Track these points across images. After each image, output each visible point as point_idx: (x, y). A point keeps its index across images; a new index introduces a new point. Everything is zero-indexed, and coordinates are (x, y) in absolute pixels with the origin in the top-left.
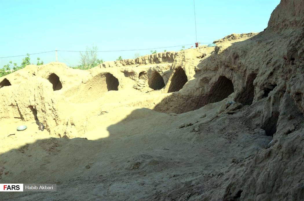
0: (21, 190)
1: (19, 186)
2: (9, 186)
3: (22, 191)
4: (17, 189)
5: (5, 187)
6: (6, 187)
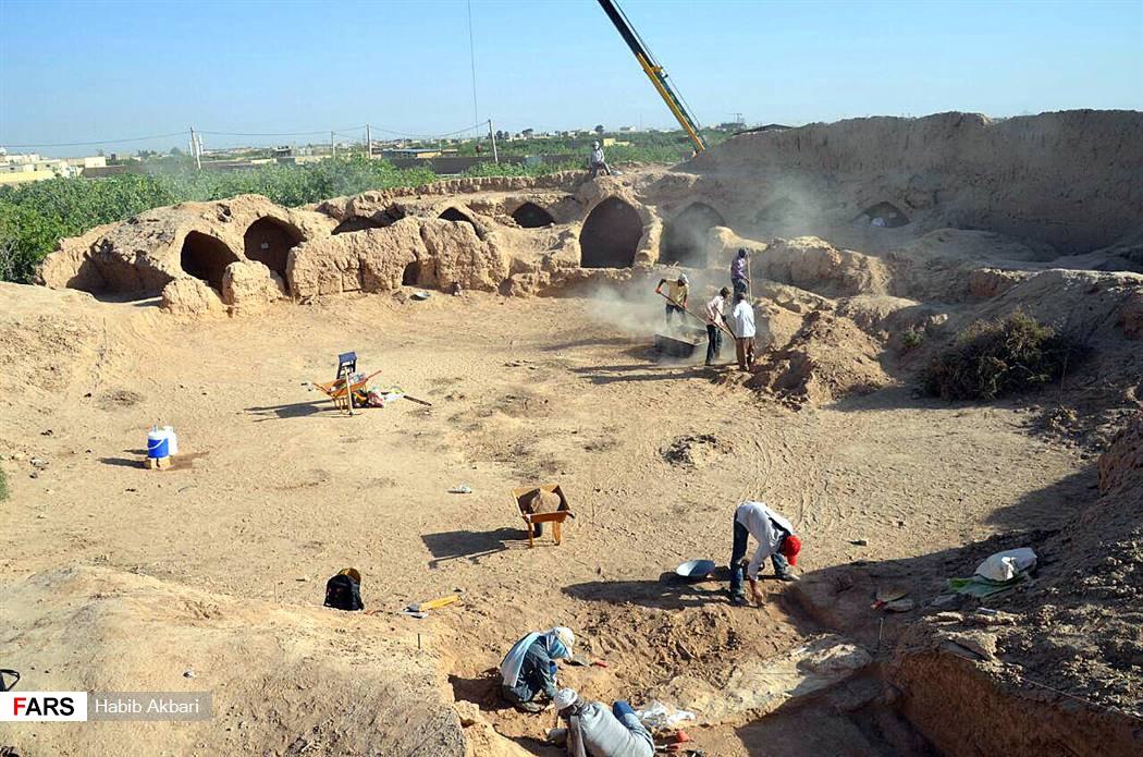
1: (71, 701)
2: (34, 700)
4: (62, 712)
5: (19, 703)
6: (23, 706)
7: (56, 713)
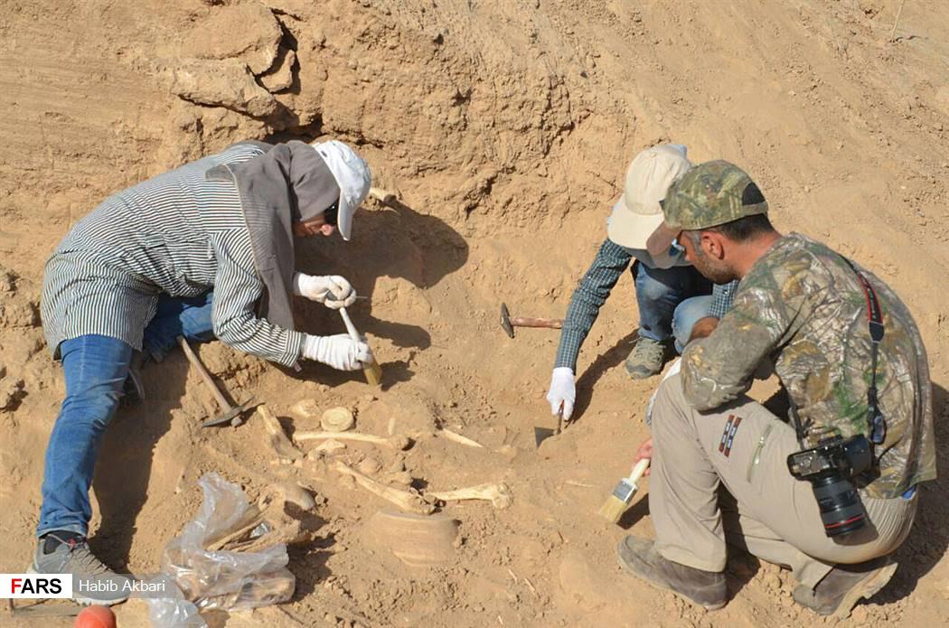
1: (59, 582)
2: (28, 581)
4: (52, 590)
5: (16, 583)
6: (19, 586)
7: (47, 592)
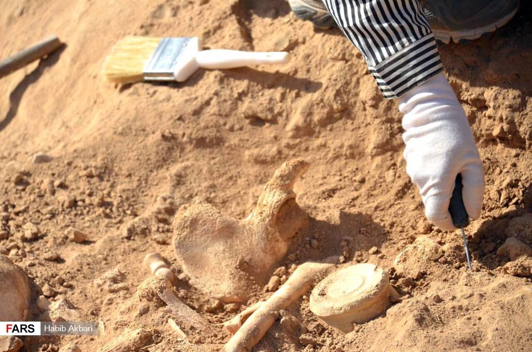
0: (37, 332)
2: (16, 326)
3: (39, 334)
4: (29, 331)
5: (9, 327)
7: (26, 332)
